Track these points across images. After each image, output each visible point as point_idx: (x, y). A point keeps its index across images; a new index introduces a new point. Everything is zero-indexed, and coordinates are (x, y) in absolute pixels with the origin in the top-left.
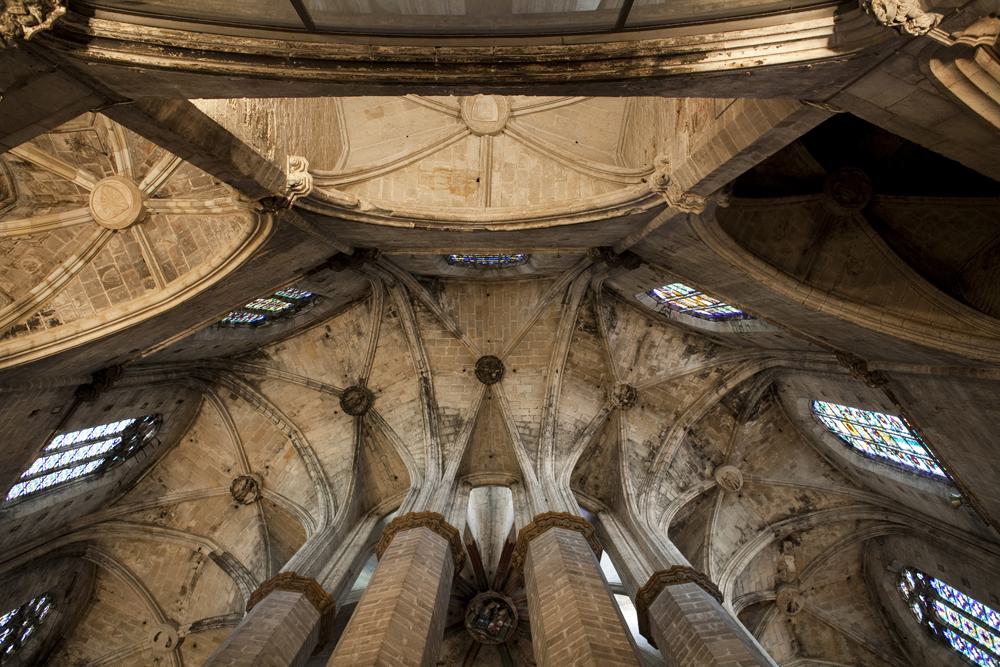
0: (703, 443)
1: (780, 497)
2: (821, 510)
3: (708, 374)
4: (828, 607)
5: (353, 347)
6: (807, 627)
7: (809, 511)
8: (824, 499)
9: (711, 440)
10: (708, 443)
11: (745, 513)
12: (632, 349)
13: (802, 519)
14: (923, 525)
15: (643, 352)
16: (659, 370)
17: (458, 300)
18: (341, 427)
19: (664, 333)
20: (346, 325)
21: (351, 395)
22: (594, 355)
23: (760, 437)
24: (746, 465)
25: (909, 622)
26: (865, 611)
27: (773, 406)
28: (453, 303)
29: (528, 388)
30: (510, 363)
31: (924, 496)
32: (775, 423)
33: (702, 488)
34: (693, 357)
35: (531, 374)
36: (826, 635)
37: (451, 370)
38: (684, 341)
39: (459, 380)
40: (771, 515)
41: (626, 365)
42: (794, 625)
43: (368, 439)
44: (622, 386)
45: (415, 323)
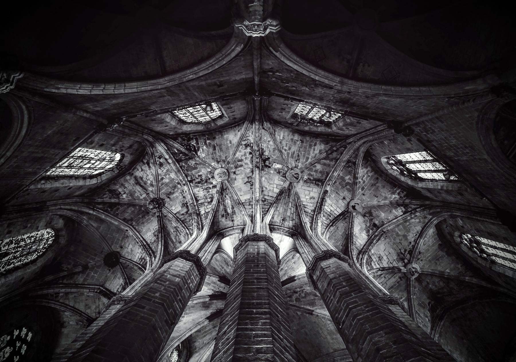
0: (200, 178)
3: (160, 162)
4: (308, 158)
5: (71, 316)
6: (312, 173)
8: (248, 138)
9: (200, 174)
10: (201, 176)
11: (243, 175)
12: (138, 188)
15: (142, 184)
19: (138, 170)
22: (130, 208)
23: (211, 150)
26: (318, 142)
27: (198, 137)
29: (131, 246)
30: (115, 248)
32: (208, 139)
33: (217, 190)
36: (319, 167)
37: (106, 276)
38: (144, 164)
40: (249, 163)
41: (144, 195)
42: (308, 178)
44: (149, 203)
45: (67, 286)
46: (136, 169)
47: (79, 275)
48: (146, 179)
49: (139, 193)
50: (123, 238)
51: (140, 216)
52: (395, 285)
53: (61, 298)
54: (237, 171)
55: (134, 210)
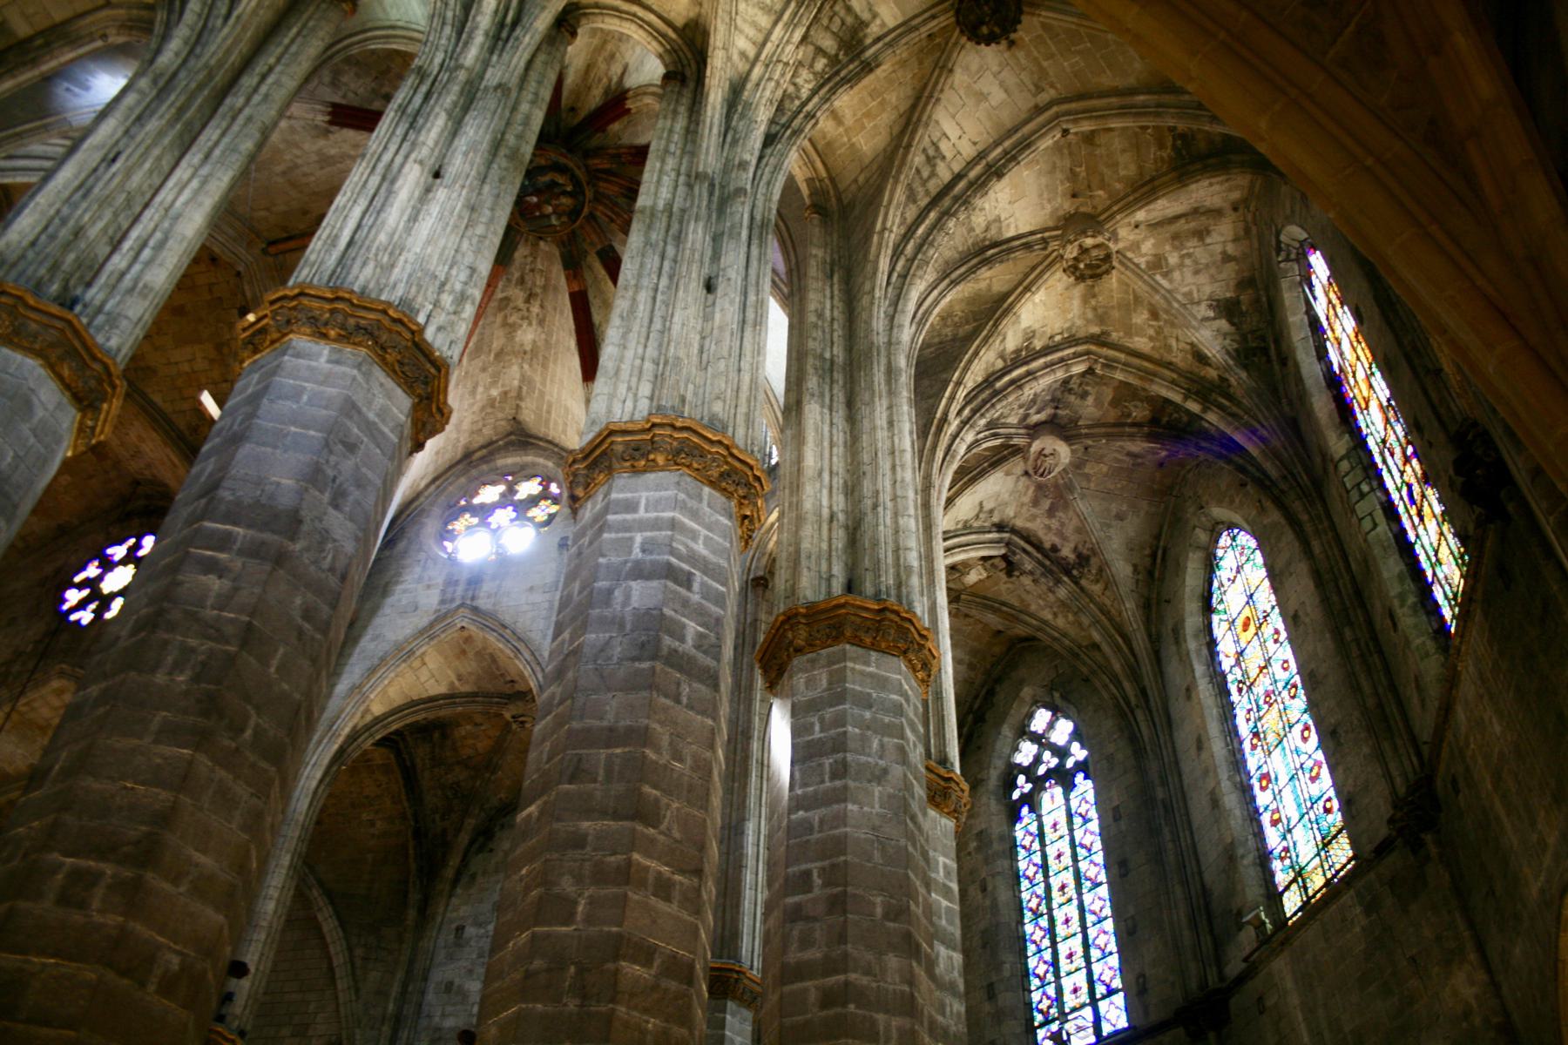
1: (1063, 524)
2: (1082, 589)
7: (1068, 573)
9: (1090, 400)
10: (1084, 395)
13: (1051, 572)
14: (1164, 783)
15: (1181, 225)
16: (1166, 275)
19: (1236, 240)
24: (1079, 454)
25: (1002, 745)
29: (997, 95)
31: (1215, 803)
34: (1223, 324)
35: (1025, 76)
40: (1029, 525)
46: (1242, 233)
48: (1189, 255)
50: (1043, 72)
51: (1081, 171)
52: (498, 669)
54: (1028, 482)
55: (1117, 172)
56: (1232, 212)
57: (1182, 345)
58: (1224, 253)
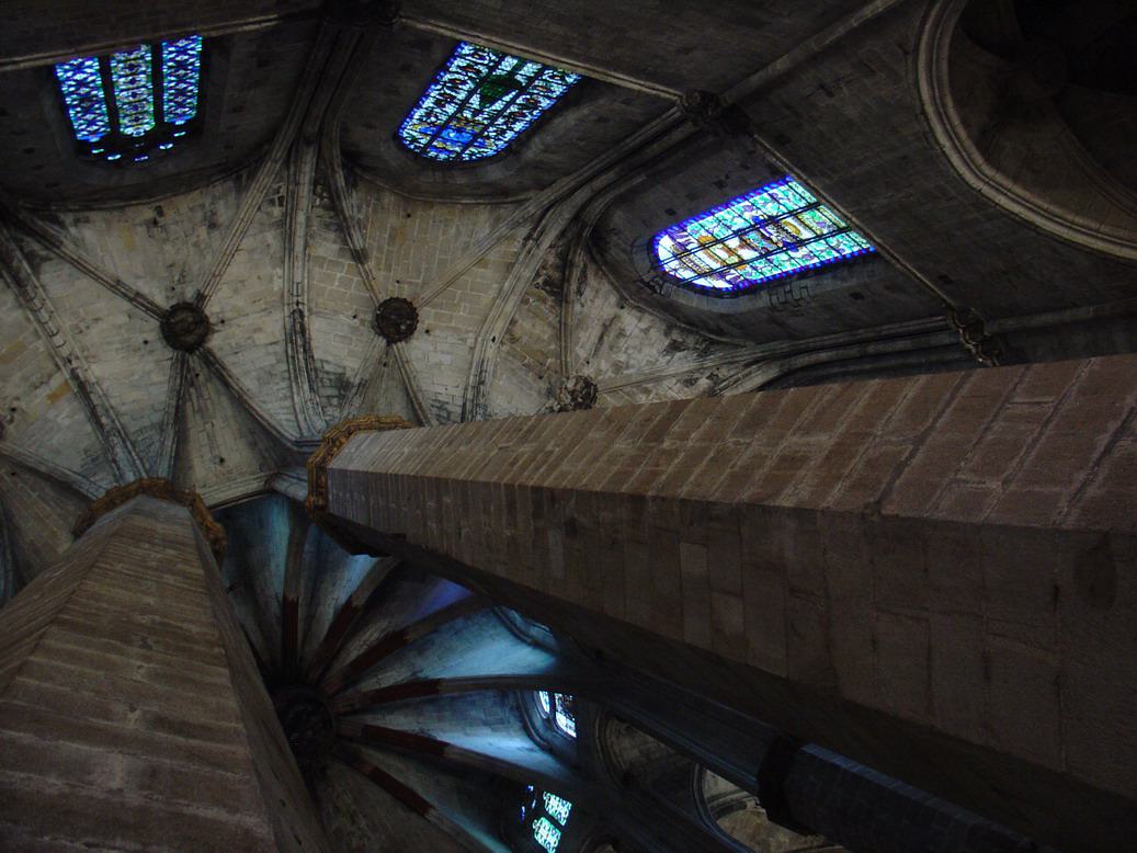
12: (595, 332)
16: (628, 367)
17: (370, 210)
18: (150, 366)
19: (640, 320)
20: (191, 209)
21: (181, 316)
22: (546, 328)
28: (364, 211)
29: (446, 359)
30: (426, 316)
34: (679, 354)
37: (336, 312)
38: (666, 334)
39: (345, 328)
41: (582, 354)
43: (192, 390)
44: (578, 378)
46: (639, 314)
47: (335, 242)
48: (627, 348)
49: (585, 339)
50: (455, 330)
53: (267, 214)
55: (543, 341)
56: (622, 311)
57: (675, 388)
58: (642, 330)
